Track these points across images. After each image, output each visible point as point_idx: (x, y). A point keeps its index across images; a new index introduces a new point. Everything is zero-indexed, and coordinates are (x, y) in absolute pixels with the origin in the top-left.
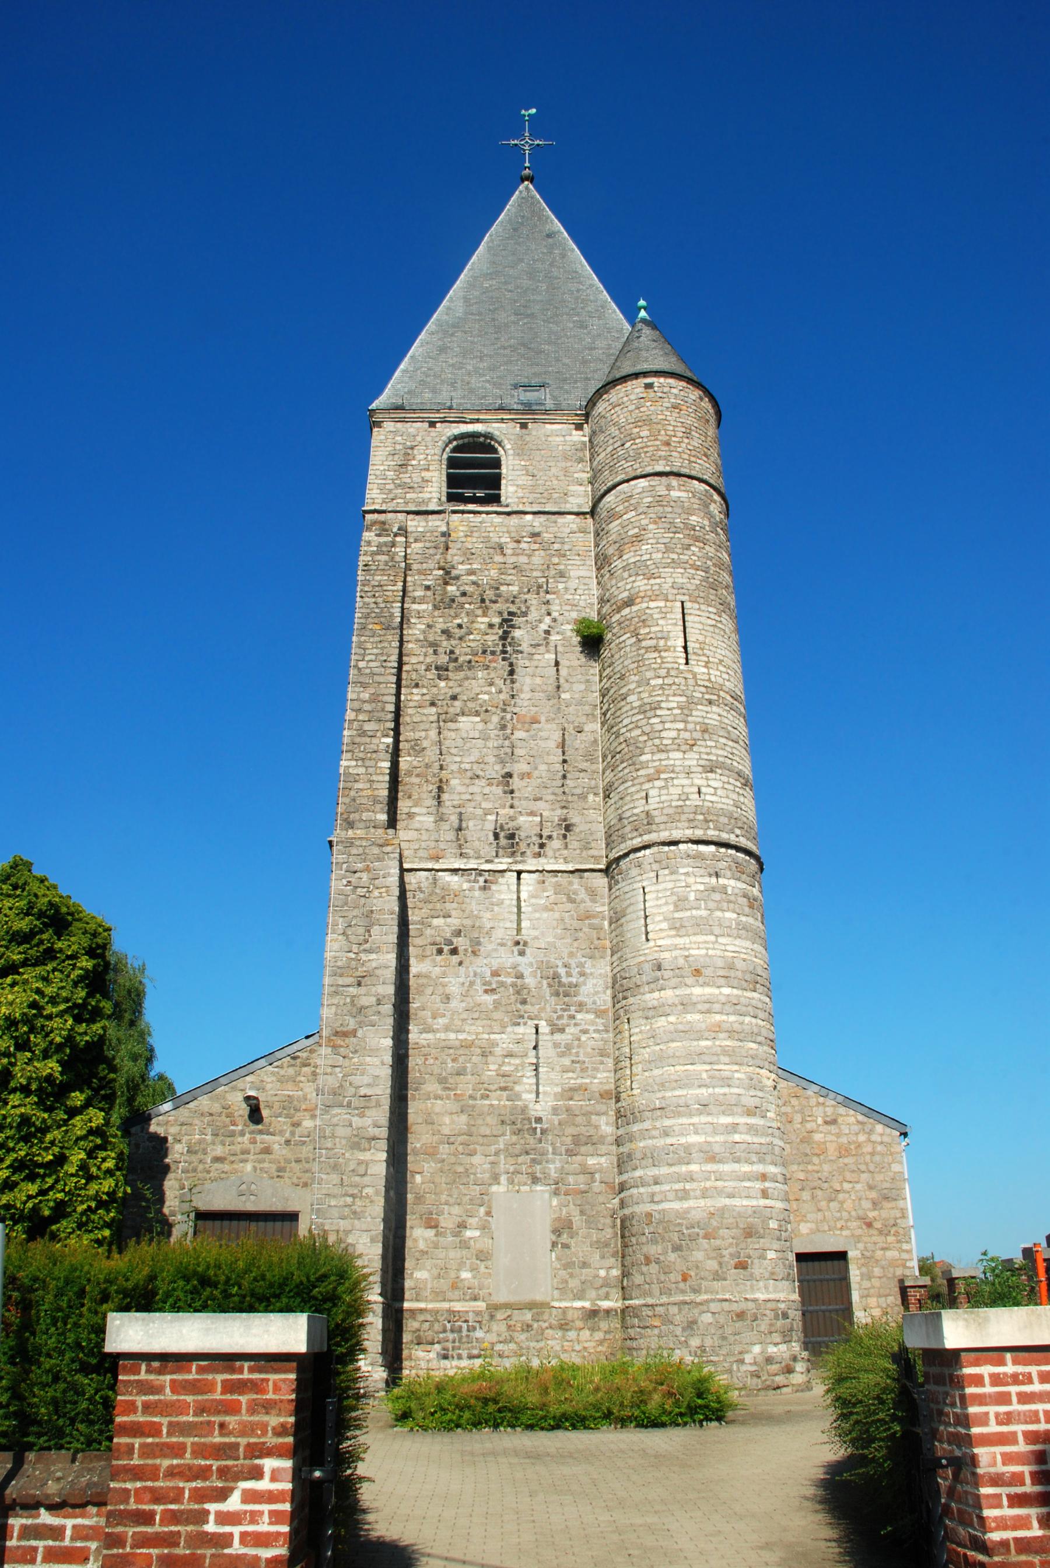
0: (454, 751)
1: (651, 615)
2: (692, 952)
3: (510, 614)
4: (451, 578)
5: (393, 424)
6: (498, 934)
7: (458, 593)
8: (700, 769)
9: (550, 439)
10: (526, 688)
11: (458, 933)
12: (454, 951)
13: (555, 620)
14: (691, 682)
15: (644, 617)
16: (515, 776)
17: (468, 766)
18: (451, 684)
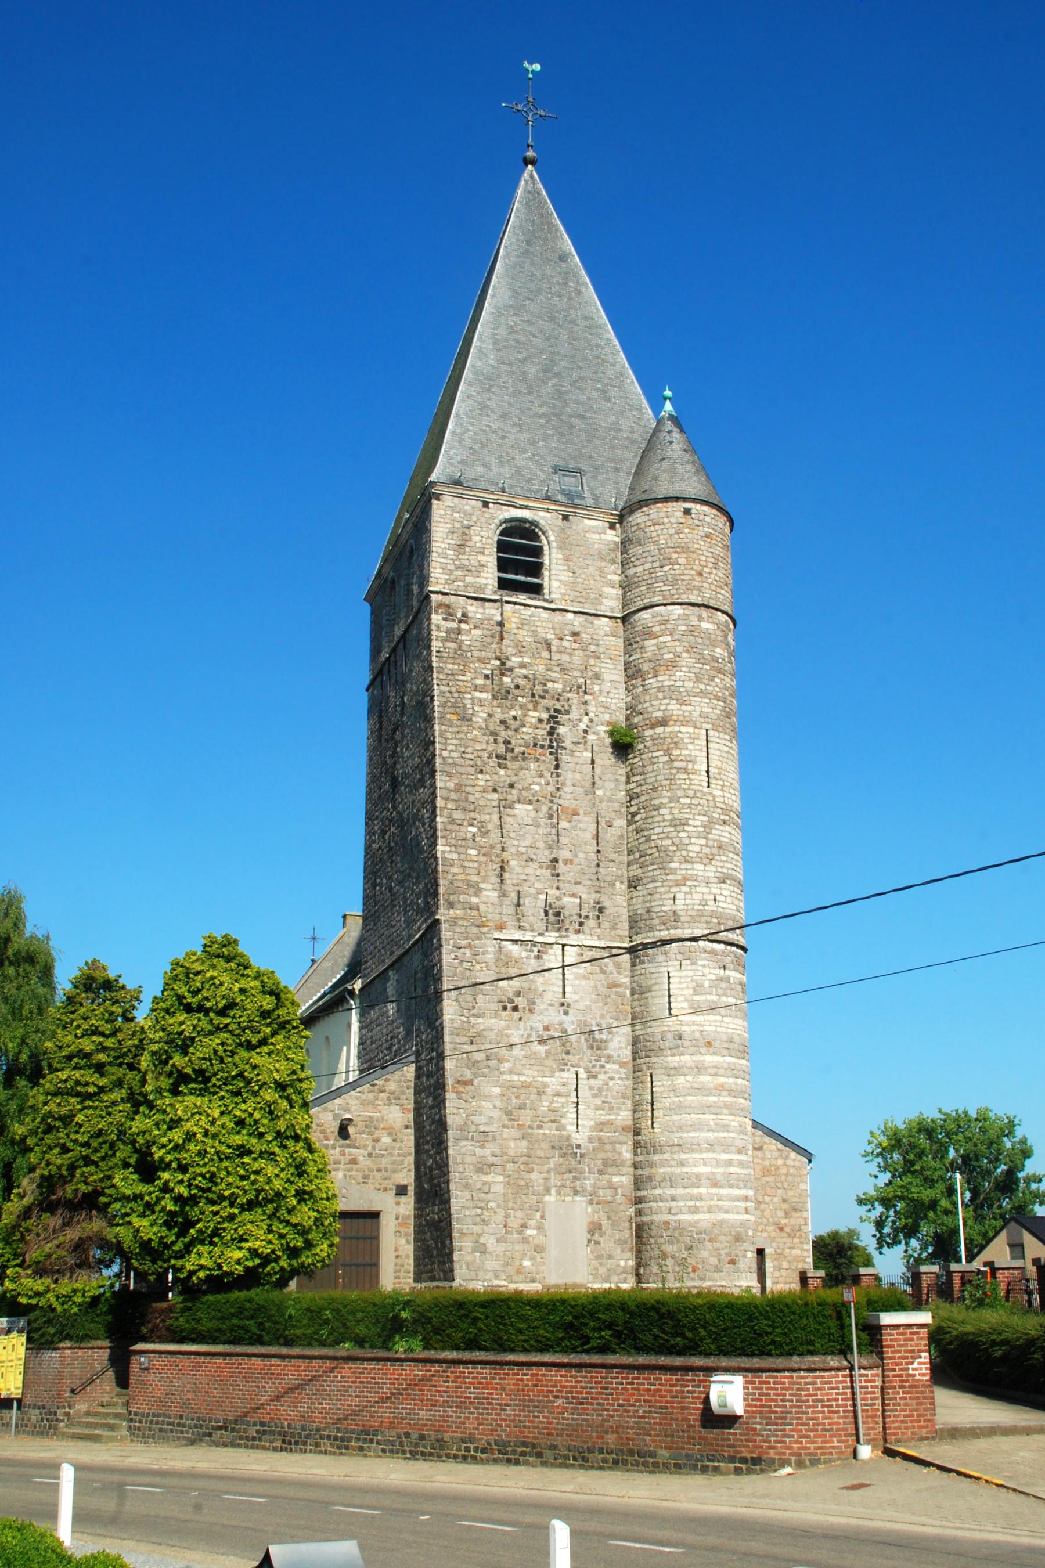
0: (512, 835)
1: (682, 739)
2: (706, 1028)
3: (556, 711)
4: (506, 670)
5: (450, 498)
6: (549, 997)
7: (512, 686)
8: (716, 880)
9: (587, 535)
10: (569, 783)
11: (518, 994)
12: (515, 1009)
13: (591, 721)
14: (711, 804)
15: (676, 740)
16: (560, 861)
17: (524, 850)
18: (509, 772)
